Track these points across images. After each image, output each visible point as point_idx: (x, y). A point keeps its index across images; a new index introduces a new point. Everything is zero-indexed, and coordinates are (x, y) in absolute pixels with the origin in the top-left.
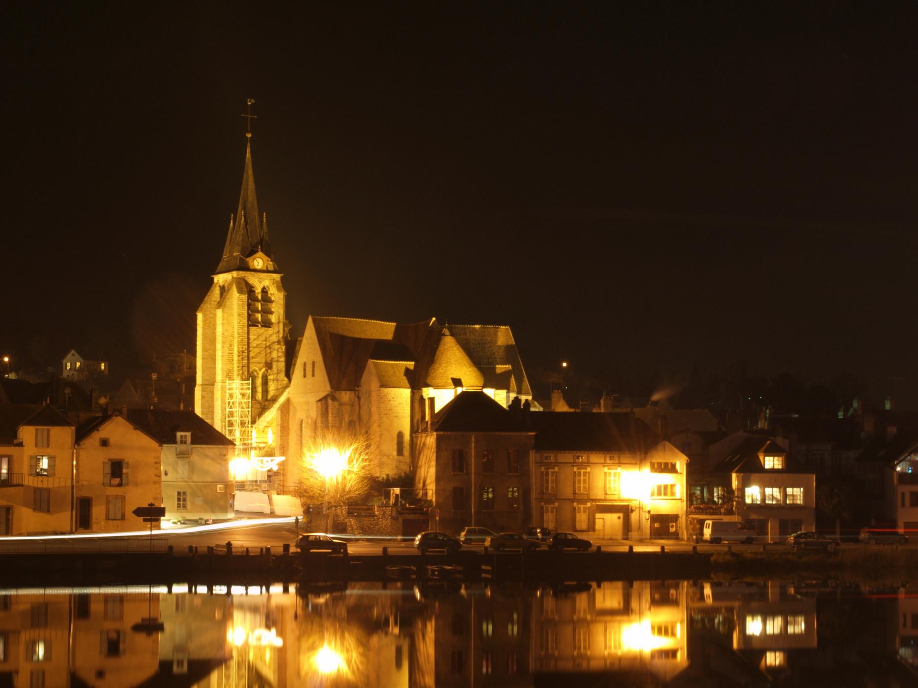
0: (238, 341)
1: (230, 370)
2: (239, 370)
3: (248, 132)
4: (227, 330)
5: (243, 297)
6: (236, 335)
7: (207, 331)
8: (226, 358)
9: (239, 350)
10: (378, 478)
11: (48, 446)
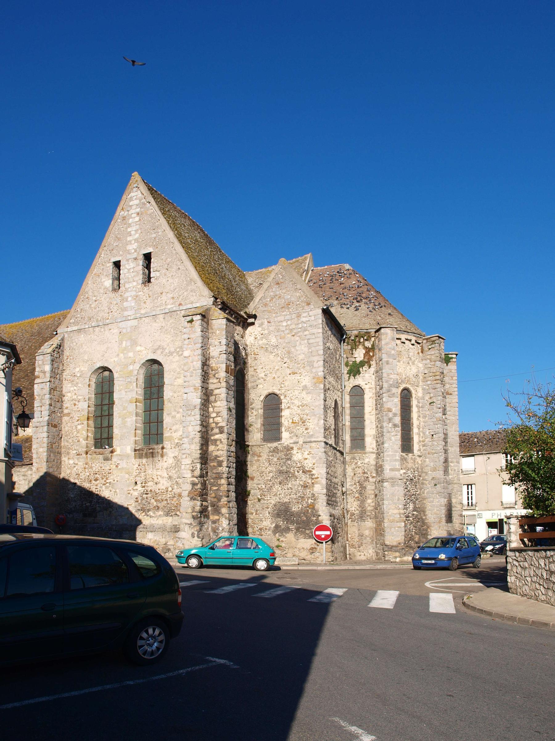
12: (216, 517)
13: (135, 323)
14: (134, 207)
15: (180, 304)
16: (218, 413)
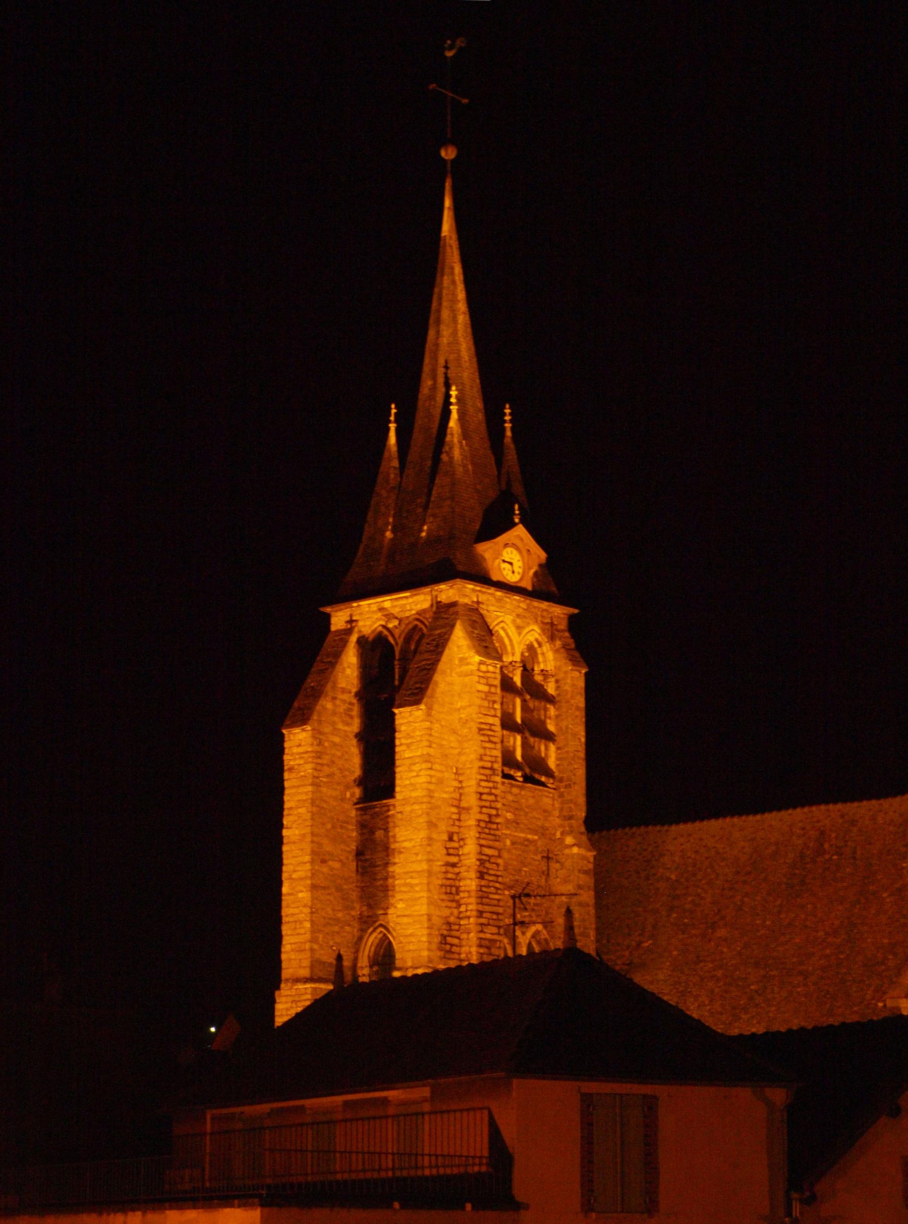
0: (479, 821)
1: (449, 924)
2: (481, 924)
3: (444, 143)
4: (440, 782)
5: (491, 669)
7: (324, 790)
8: (440, 882)
9: (481, 853)
11: (651, 1207)
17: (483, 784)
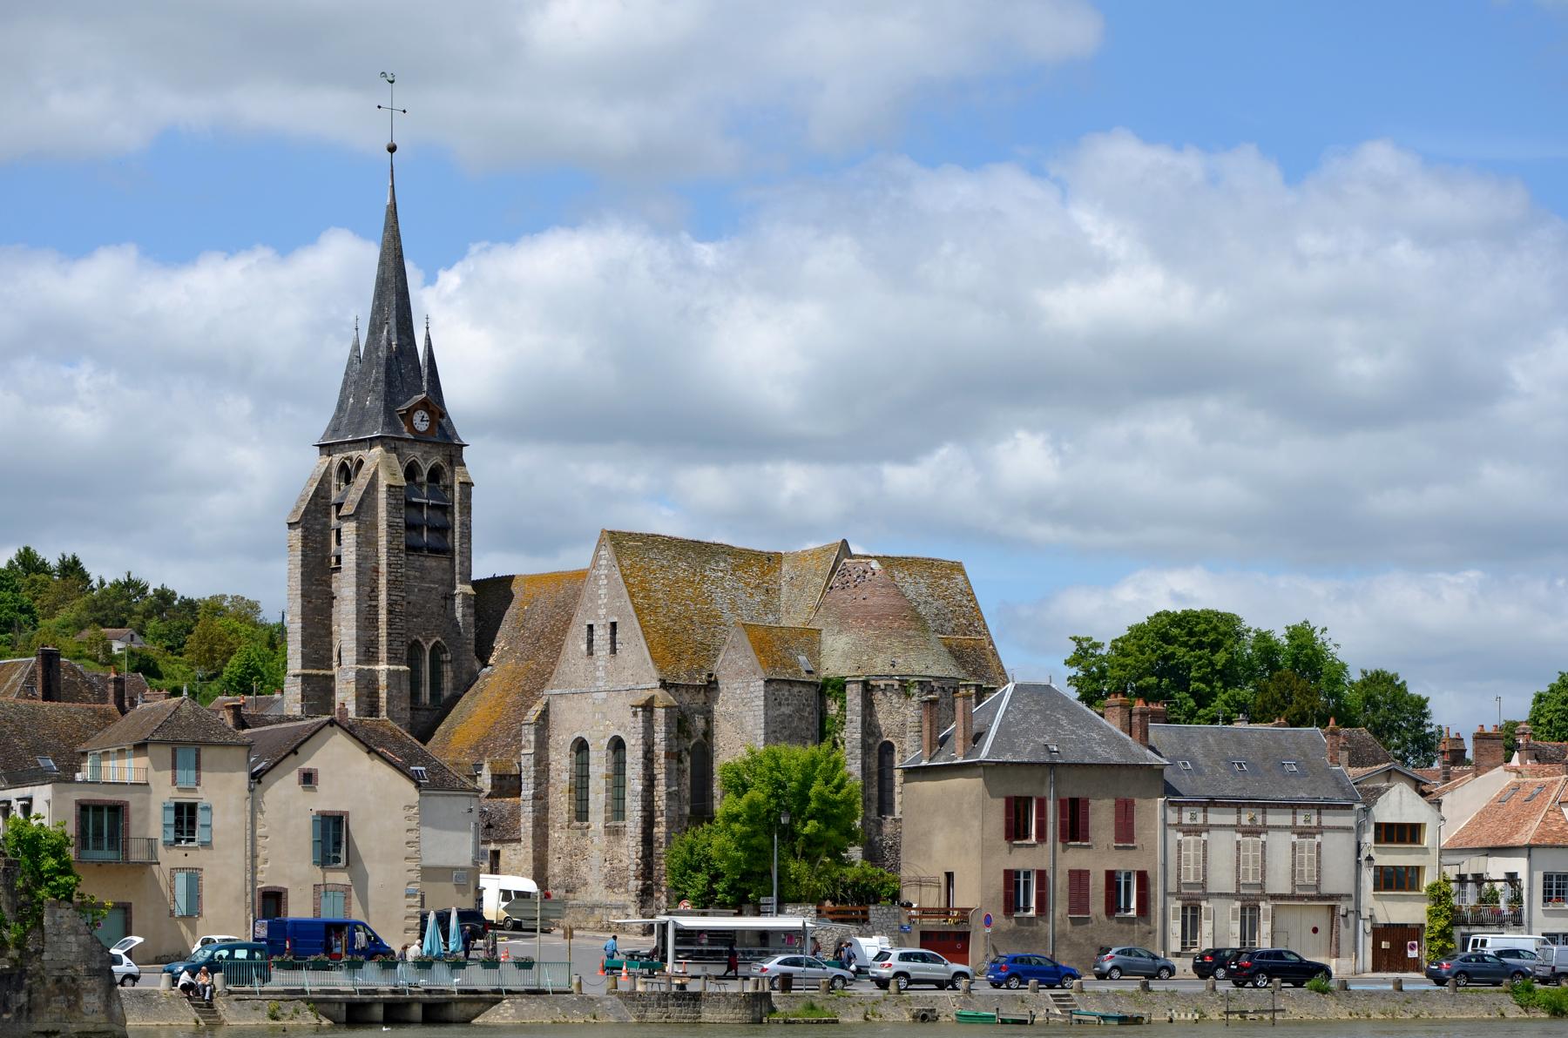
6: (383, 568)
10: (638, 865)
12: (659, 895)
13: (604, 695)
14: (603, 567)
15: (637, 683)
16: (659, 797)
17: (392, 558)
